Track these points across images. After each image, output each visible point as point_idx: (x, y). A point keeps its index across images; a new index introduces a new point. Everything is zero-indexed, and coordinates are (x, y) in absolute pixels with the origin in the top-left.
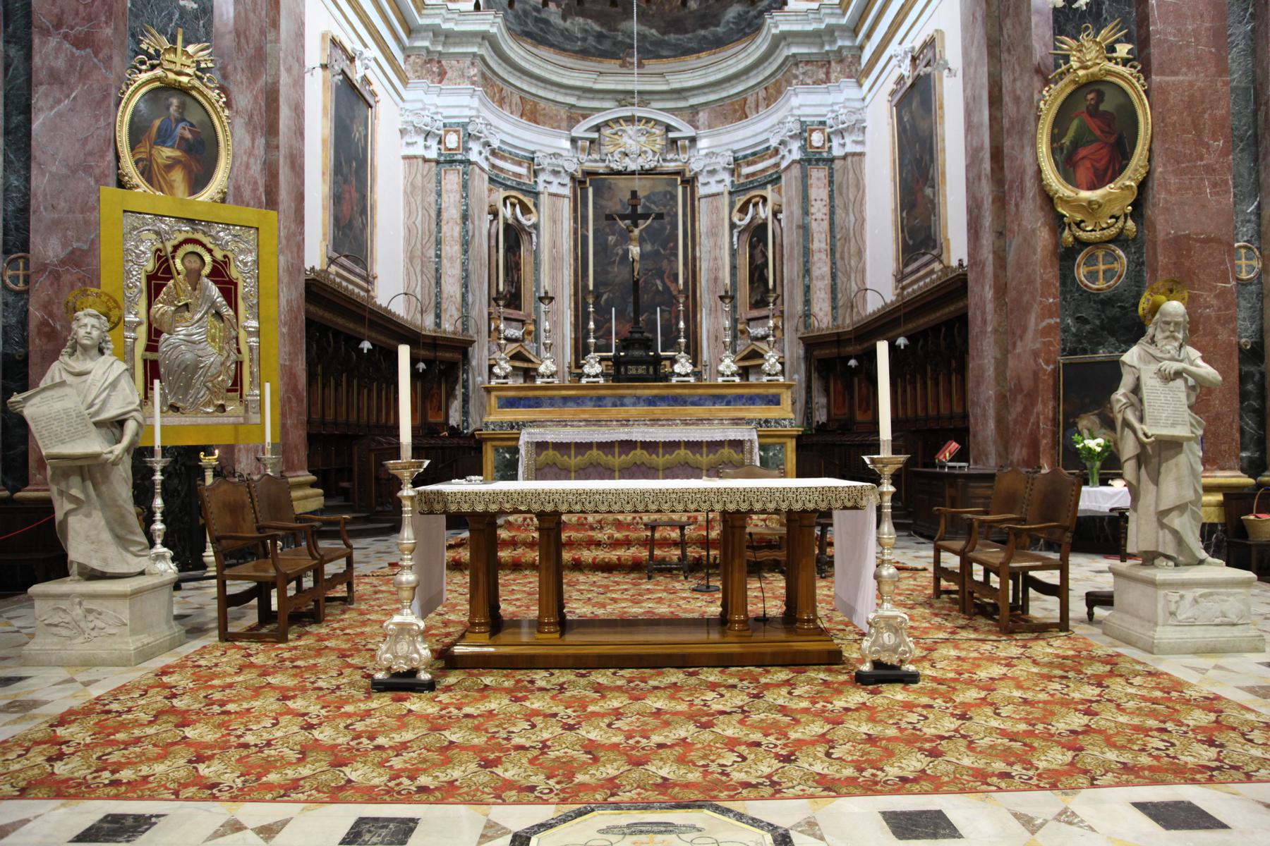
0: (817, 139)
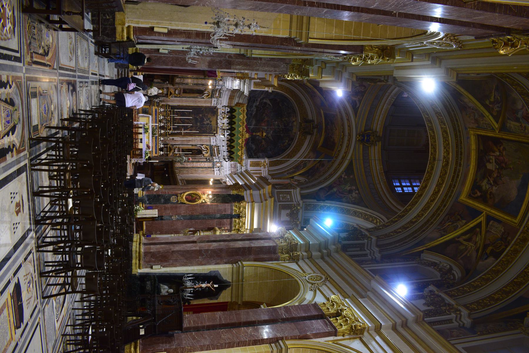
0: (218, 165)
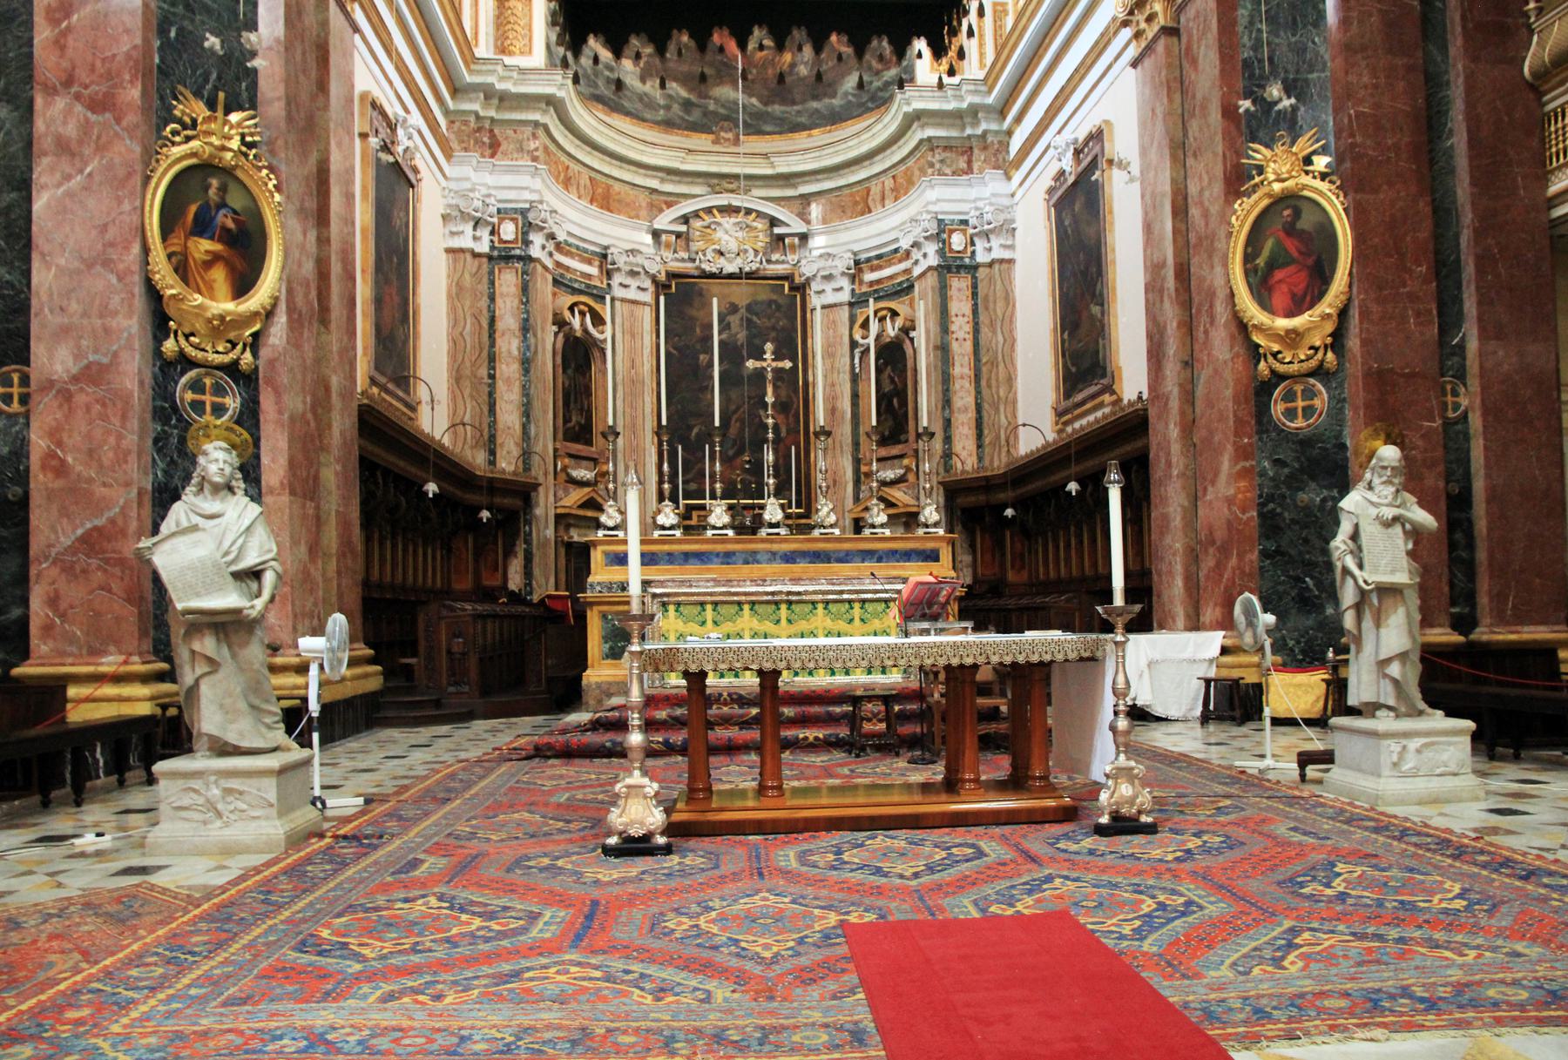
0: (957, 242)
